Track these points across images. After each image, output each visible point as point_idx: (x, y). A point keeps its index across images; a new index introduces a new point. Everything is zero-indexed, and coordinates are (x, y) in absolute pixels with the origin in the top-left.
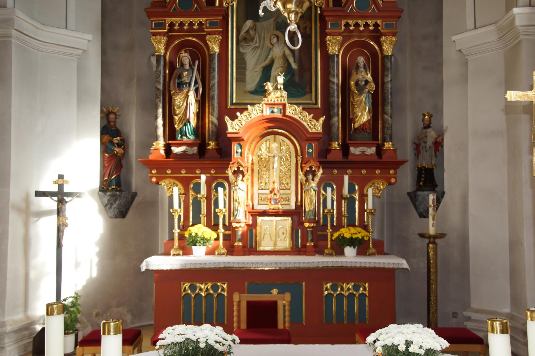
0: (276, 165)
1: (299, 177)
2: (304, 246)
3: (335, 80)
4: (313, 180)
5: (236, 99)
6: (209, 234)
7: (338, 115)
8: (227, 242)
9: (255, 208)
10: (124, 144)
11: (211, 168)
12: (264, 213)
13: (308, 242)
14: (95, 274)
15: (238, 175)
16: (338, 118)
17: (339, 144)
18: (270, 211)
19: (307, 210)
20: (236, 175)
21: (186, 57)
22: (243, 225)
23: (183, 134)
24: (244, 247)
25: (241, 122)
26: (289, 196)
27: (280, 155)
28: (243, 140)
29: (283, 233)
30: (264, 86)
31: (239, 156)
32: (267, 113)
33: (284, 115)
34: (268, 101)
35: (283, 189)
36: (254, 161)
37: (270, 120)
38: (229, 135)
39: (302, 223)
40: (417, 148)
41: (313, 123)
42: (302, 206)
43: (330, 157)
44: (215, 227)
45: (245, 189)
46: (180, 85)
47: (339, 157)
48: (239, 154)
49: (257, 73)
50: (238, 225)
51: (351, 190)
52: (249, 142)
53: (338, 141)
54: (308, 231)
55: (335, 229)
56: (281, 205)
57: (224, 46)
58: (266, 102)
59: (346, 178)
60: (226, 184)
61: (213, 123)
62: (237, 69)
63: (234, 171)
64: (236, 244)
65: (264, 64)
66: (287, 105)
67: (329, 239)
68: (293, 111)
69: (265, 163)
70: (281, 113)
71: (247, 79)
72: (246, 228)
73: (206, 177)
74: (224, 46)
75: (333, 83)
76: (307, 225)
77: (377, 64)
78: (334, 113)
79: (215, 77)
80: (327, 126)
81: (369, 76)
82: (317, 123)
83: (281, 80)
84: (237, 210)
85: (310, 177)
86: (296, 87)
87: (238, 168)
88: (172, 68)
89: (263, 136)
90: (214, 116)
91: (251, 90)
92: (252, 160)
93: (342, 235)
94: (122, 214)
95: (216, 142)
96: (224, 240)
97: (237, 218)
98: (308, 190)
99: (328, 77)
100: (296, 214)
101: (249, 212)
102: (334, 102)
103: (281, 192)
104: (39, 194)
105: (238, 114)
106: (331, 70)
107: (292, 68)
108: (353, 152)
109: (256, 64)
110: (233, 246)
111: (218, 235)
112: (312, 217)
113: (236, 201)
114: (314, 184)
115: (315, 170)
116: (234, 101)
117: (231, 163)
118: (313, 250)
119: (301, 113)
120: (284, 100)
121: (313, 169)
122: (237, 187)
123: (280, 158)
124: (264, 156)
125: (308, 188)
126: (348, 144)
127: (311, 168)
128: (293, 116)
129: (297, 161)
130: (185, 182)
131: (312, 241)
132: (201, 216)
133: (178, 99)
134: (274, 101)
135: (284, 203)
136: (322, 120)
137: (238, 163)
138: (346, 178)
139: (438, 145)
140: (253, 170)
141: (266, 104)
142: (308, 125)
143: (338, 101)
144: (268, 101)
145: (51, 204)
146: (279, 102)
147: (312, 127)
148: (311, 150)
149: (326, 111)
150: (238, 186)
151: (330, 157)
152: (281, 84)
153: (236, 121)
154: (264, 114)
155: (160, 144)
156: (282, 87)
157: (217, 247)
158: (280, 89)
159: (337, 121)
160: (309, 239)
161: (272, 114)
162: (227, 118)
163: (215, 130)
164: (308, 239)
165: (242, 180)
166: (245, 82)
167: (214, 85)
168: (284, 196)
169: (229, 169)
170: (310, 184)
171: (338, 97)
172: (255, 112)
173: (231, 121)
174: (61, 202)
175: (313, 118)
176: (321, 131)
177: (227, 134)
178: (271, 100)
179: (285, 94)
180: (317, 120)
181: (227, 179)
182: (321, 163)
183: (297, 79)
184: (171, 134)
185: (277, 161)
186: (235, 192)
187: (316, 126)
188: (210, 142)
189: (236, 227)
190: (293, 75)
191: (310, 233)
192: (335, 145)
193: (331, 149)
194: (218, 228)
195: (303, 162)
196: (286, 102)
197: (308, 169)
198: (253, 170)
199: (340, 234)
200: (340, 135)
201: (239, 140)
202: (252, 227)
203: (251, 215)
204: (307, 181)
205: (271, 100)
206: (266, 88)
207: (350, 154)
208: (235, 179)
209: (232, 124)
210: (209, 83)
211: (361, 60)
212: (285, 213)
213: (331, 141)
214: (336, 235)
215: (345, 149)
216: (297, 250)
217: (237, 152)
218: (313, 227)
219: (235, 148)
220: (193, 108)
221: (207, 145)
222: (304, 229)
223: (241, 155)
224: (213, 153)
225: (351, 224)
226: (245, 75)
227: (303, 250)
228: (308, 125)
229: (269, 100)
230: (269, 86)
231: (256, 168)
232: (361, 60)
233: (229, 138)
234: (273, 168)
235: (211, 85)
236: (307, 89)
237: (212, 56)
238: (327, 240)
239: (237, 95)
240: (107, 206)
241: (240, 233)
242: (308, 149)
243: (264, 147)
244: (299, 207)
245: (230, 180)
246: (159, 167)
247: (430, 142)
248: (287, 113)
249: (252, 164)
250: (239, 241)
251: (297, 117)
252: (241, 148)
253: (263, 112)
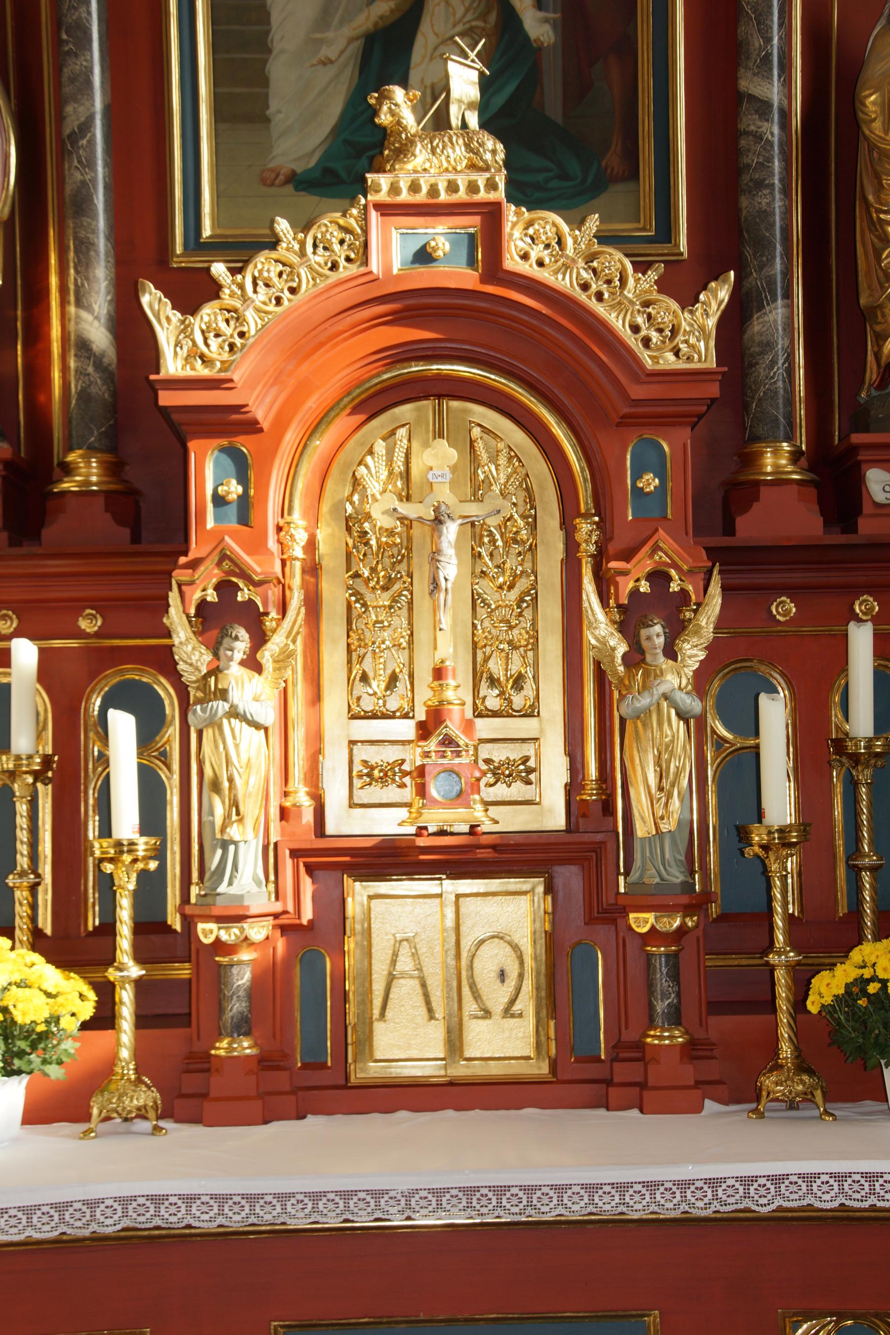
0: (451, 569)
1: (590, 638)
2: (631, 1050)
3: (774, 92)
4: (671, 652)
5: (216, 222)
7: (788, 295)
8: (171, 1039)
9: (331, 828)
11: (77, 606)
12: (388, 859)
13: (651, 1023)
15: (224, 634)
16: (790, 307)
17: (796, 456)
18: (421, 842)
19: (641, 830)
20: (214, 633)
22: (258, 931)
24: (268, 1062)
25: (235, 315)
26: (529, 750)
27: (473, 510)
28: (252, 427)
29: (502, 975)
30: (375, 112)
31: (234, 525)
32: (392, 250)
33: (493, 269)
34: (394, 189)
35: (495, 714)
36: (323, 548)
37: (411, 305)
38: (166, 399)
39: (608, 913)
41: (665, 319)
42: (608, 807)
43: (752, 527)
45: (268, 715)
47: (805, 523)
48: (232, 511)
49: (326, 74)
50: (229, 935)
52: (291, 438)
53: (789, 438)
54: (649, 956)
56: (487, 804)
58: (383, 196)
60: (165, 690)
61: (84, 346)
62: (216, 47)
63: (203, 605)
64: (222, 1048)
65: (366, 20)
66: (510, 212)
67: (783, 1004)
68: (542, 246)
69: (392, 564)
70: (472, 262)
71: (274, 104)
72: (281, 944)
73: (42, 651)
75: (763, 107)
76: (642, 922)
78: (771, 282)
79: (89, 83)
82: (685, 320)
84: (225, 845)
85: (656, 634)
86: (556, 140)
87: (225, 588)
89: (373, 403)
90: (89, 309)
91: (299, 168)
92: (311, 546)
93: (873, 988)
95: (107, 457)
96: (142, 1021)
97: (222, 888)
98: (642, 716)
99: (734, 79)
100: (578, 859)
101: (295, 854)
102: (766, 215)
103: (485, 727)
105: (219, 269)
106: (747, 30)
107: (527, 37)
108: (880, 496)
109: (323, 20)
110: (201, 1062)
111: (106, 994)
112: (677, 876)
113: (216, 787)
114: (674, 680)
115: (683, 592)
116: (207, 231)
117: (183, 560)
118: (688, 1073)
119: (590, 258)
120: (491, 185)
121: (674, 587)
122: (221, 707)
123: (475, 530)
124: (383, 521)
125: (644, 701)
126: (855, 449)
127: (658, 577)
128: (544, 275)
129: (571, 546)
131: (675, 1018)
132: (11, 881)
134: (433, 191)
135: (501, 791)
136: (720, 294)
137: (223, 557)
140: (313, 605)
141: (385, 209)
142: (636, 329)
143: (787, 213)
144: (394, 189)
146: (462, 195)
147: (655, 336)
150: (223, 694)
151: (752, 527)
152: (471, 106)
153: (208, 311)
154: (375, 265)
156: (473, 120)
157: (100, 1076)
158: (464, 125)
160: (661, 1006)
161: (422, 269)
162: (151, 299)
163: (100, 389)
164: (651, 1007)
165: (253, 664)
166: (268, 120)
167: (86, 127)
168: (499, 753)
169: (174, 597)
170: (652, 675)
171: (786, 191)
172: (319, 258)
173: (176, 316)
175: (663, 286)
176: (712, 363)
177: (153, 389)
178: (414, 188)
179: (493, 149)
180: (688, 300)
181: (165, 661)
182: (713, 553)
183: (553, 104)
185: (458, 546)
186: (208, 734)
187: (682, 337)
188: (71, 457)
189: (219, 946)
190: (532, 81)
192: (775, 460)
193: (757, 484)
194: (110, 960)
195: (612, 548)
196: (500, 194)
197: (644, 587)
198: (313, 605)
199: (863, 982)
200: (801, 412)
201: (228, 423)
202: (316, 940)
203: (310, 870)
204: (636, 657)
205: (414, 188)
206: (384, 118)
207: (867, 508)
208: (208, 657)
209: (185, 330)
210: (60, 118)
213: (756, 439)
214: (827, 987)
216: (592, 1070)
217: (219, 501)
218: (682, 931)
219: (210, 471)
221: (57, 471)
223: (244, 519)
226: (265, 82)
227: (623, 1072)
228: (636, 329)
229: (404, 185)
230: (400, 107)
231: (334, 595)
233: (165, 412)
234: (435, 585)
235: (67, 131)
236: (613, 160)
238: (771, 1007)
239: (218, 196)
241: (242, 979)
242: (637, 475)
243: (375, 475)
244: (596, 808)
245: (181, 666)
248: (512, 262)
249: (313, 569)
250: (243, 1027)
251: (564, 283)
252: (243, 480)
253: (366, 262)
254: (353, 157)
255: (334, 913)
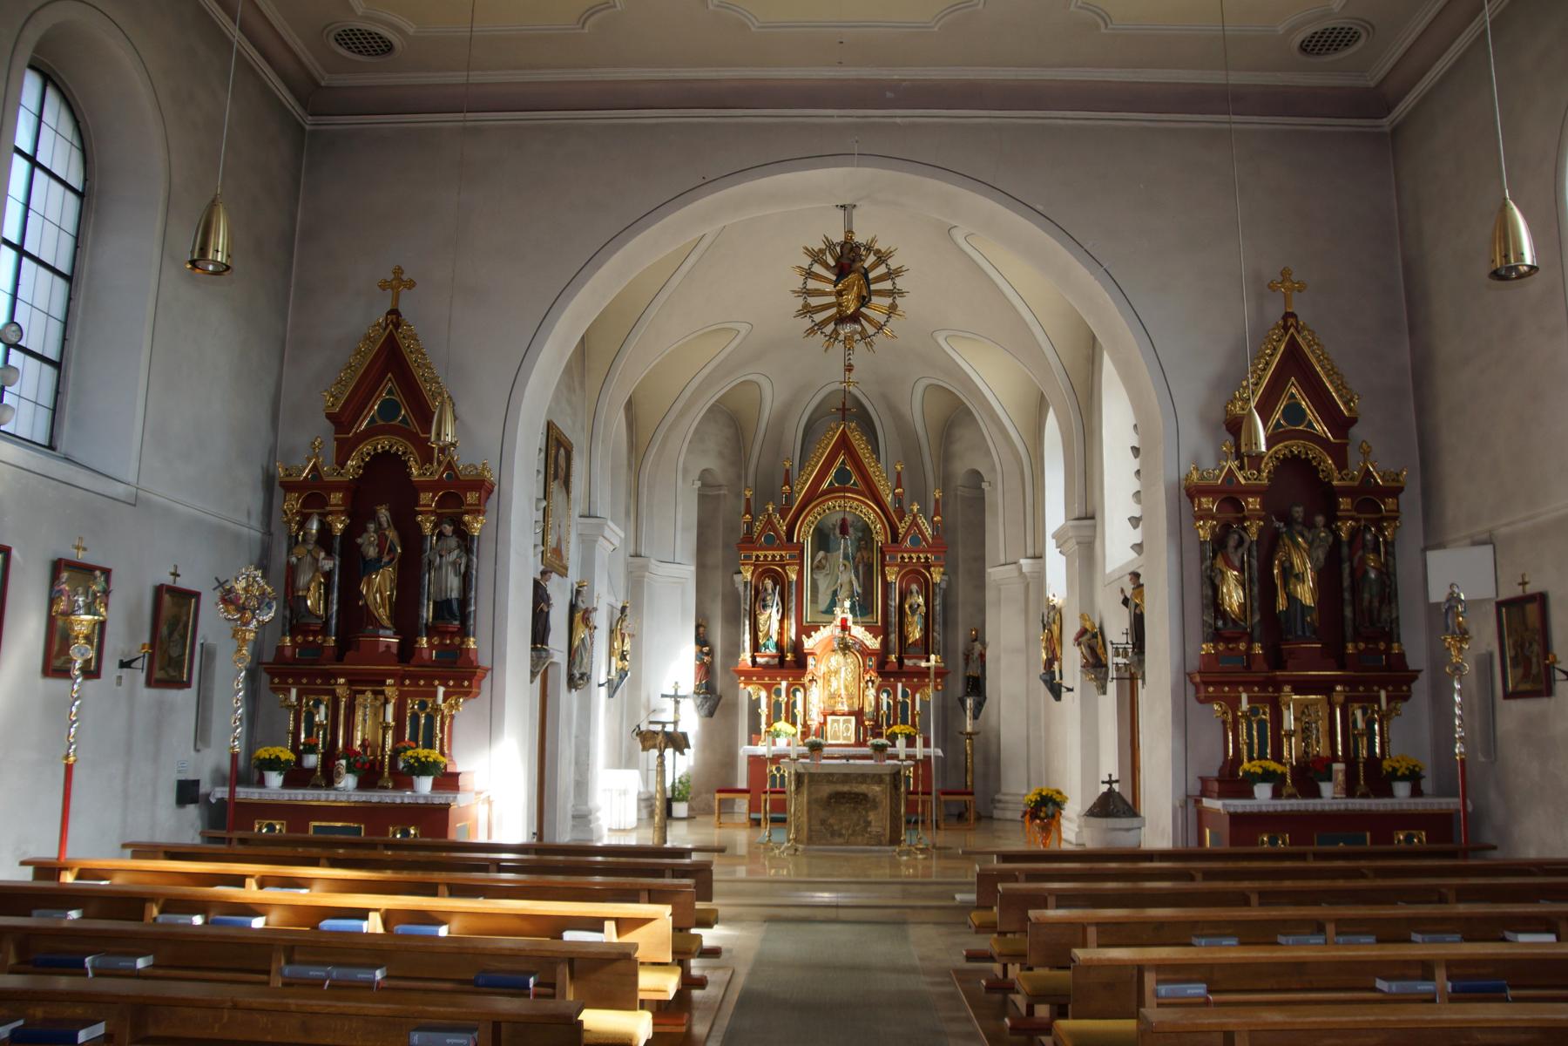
6: (791, 730)
10: (711, 653)
12: (833, 714)
14: (692, 763)
21: (769, 583)
23: (767, 647)
40: (967, 658)
43: (888, 668)
44: (794, 724)
46: (765, 607)
51: (905, 694)
55: (889, 726)
57: (800, 574)
59: (900, 686)
74: (800, 574)
77: (927, 588)
80: (885, 643)
81: (921, 600)
83: (847, 604)
86: (863, 607)
88: (757, 592)
94: (711, 714)
100: (859, 714)
104: (663, 696)
130: (768, 687)
133: (762, 619)
138: (900, 686)
139: (982, 656)
145: (670, 703)
148: (872, 662)
149: (881, 630)
151: (888, 668)
155: (746, 656)
159: (894, 637)
174: (677, 702)
184: (756, 647)
187: (873, 643)
191: (870, 726)
192: (893, 658)
211: (914, 587)
212: (850, 714)
215: (900, 660)
219: (810, 660)
220: (775, 626)
222: (865, 727)
224: (792, 662)
225: (904, 722)
232: (914, 587)
237: (790, 583)
240: (699, 707)
246: (748, 676)
247: (976, 655)
254: (830, 611)
255: (825, 723)
